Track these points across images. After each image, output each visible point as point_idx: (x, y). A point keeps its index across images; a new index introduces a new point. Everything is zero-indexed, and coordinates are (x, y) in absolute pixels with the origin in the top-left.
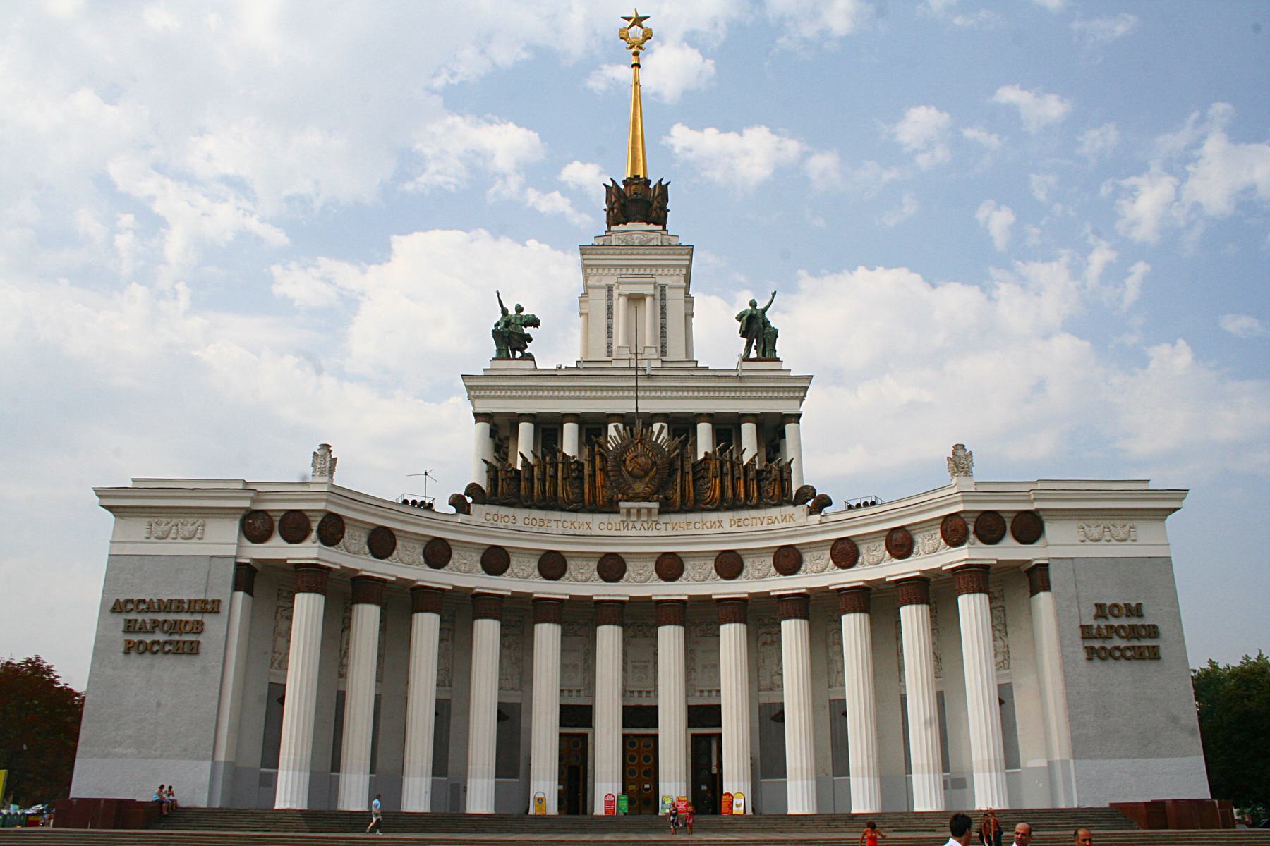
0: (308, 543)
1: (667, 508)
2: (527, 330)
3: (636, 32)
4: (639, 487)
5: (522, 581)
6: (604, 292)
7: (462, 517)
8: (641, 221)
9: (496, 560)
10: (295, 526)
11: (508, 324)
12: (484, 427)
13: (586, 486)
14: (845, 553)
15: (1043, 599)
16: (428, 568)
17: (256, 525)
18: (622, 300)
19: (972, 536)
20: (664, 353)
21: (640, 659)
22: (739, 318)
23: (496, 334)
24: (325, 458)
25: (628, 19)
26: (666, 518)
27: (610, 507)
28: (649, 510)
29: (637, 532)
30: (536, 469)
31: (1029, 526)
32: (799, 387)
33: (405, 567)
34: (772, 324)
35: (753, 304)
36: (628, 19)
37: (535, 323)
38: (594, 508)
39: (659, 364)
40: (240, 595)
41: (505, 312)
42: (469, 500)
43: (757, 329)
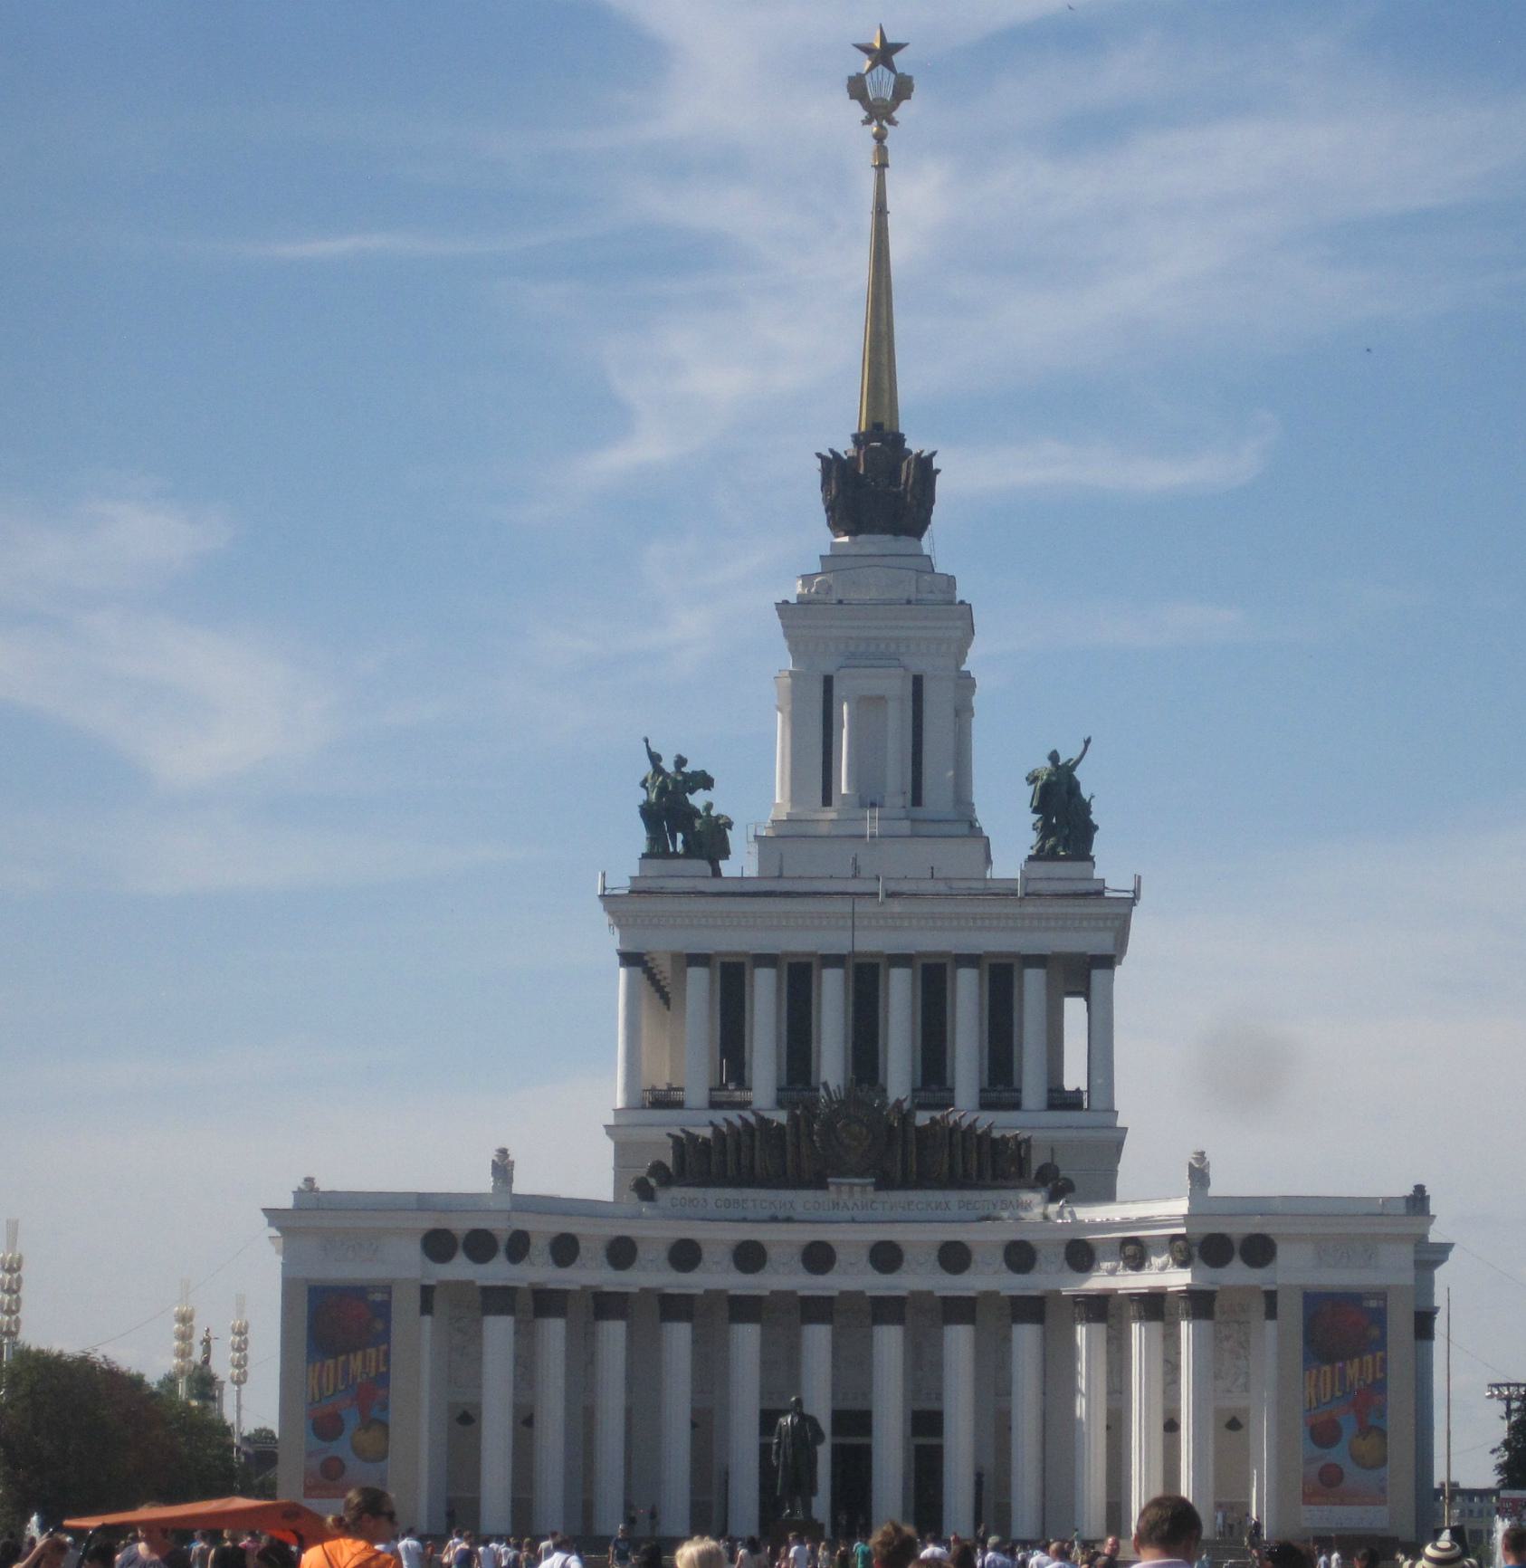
0: (495, 1260)
1: (884, 1183)
2: (698, 799)
3: (881, 84)
5: (717, 1276)
7: (645, 1208)
8: (884, 531)
9: (685, 1255)
10: (480, 1245)
11: (662, 791)
13: (789, 1157)
14: (1081, 1255)
15: (1270, 1324)
16: (610, 1268)
17: (438, 1245)
19: (1196, 1259)
20: (917, 800)
21: (853, 1364)
22: (1032, 779)
23: (648, 812)
24: (503, 1168)
25: (867, 50)
26: (883, 1195)
27: (820, 1184)
28: (863, 1186)
29: (851, 1217)
30: (729, 1140)
31: (1259, 1250)
32: (1116, 915)
33: (593, 1273)
34: (1085, 792)
36: (867, 50)
37: (705, 781)
38: (799, 1183)
40: (427, 1319)
41: (655, 759)
42: (653, 1182)
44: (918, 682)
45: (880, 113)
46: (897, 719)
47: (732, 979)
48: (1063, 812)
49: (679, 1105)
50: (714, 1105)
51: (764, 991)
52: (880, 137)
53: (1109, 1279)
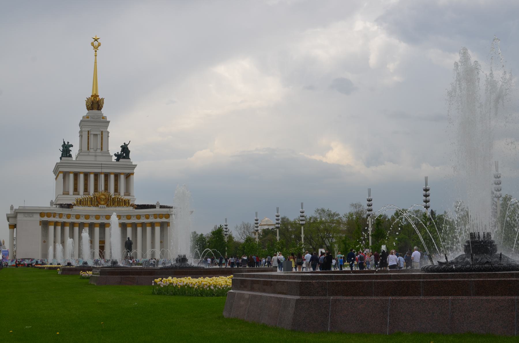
2: (71, 148)
3: (96, 43)
4: (103, 202)
6: (87, 133)
10: (49, 215)
12: (61, 175)
17: (42, 215)
18: (92, 136)
22: (121, 147)
27: (97, 206)
35: (125, 144)
37: (72, 146)
38: (94, 206)
39: (100, 154)
41: (64, 142)
43: (125, 149)
44: (102, 132)
45: (96, 48)
46: (99, 137)
47: (76, 175)
48: (125, 151)
49: (68, 194)
50: (74, 194)
51: (82, 177)
52: (96, 51)
53: (143, 220)
